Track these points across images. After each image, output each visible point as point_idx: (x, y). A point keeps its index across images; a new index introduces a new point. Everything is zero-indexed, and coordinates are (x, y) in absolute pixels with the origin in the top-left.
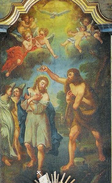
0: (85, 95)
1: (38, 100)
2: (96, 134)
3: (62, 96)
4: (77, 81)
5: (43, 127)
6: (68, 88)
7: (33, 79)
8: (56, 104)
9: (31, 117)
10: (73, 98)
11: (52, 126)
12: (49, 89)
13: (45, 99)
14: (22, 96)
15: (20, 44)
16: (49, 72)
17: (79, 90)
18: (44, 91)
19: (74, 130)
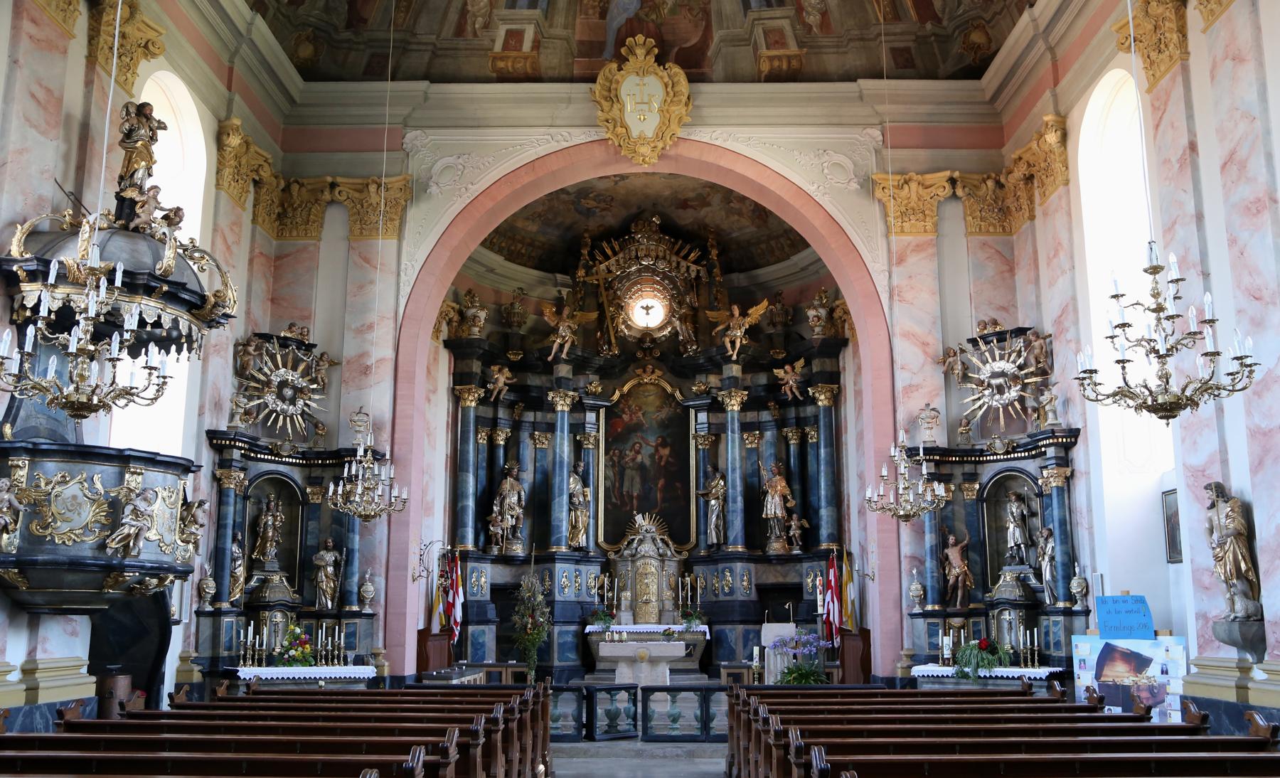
0: (670, 455)
1: (634, 460)
2: (678, 485)
3: (652, 456)
4: (664, 445)
5: (637, 480)
6: (657, 450)
7: (630, 443)
8: (647, 462)
9: (628, 472)
10: (661, 458)
11: (644, 480)
12: (643, 451)
13: (639, 458)
14: (622, 456)
15: (620, 417)
16: (642, 438)
17: (666, 452)
18: (638, 452)
19: (661, 482)
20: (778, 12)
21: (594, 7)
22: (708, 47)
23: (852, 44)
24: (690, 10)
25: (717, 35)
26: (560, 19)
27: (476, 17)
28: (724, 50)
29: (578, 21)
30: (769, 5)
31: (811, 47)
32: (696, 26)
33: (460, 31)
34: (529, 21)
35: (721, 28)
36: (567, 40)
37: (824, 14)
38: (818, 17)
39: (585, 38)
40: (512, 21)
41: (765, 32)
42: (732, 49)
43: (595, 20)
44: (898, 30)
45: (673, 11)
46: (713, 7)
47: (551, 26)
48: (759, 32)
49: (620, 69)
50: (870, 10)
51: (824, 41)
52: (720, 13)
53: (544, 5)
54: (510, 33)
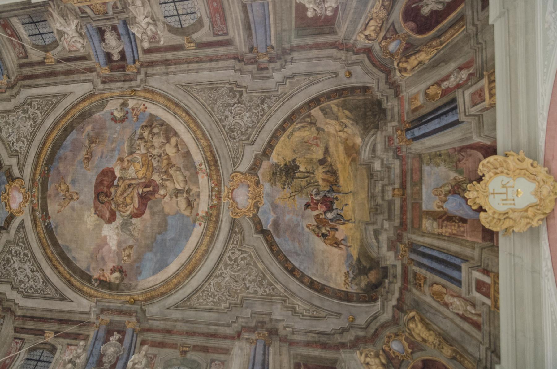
20: (460, 101)
21: (459, 227)
22: (484, 145)
23: (480, 41)
24: (459, 160)
25: (476, 140)
26: (468, 252)
27: (466, 310)
28: (486, 133)
29: (469, 239)
30: (456, 108)
31: (483, 69)
32: (470, 155)
33: (477, 326)
34: (469, 274)
35: (471, 138)
36: (482, 249)
37: (460, 69)
38: (463, 72)
39: (481, 236)
40: (469, 285)
41: (474, 106)
42: (485, 127)
43: (467, 227)
44: (470, 13)
45: (461, 172)
46: (457, 145)
47: (473, 259)
48: (473, 111)
49: (485, 211)
50: (457, 39)
51: (479, 61)
52: (461, 140)
53: (460, 260)
54: (478, 289)
